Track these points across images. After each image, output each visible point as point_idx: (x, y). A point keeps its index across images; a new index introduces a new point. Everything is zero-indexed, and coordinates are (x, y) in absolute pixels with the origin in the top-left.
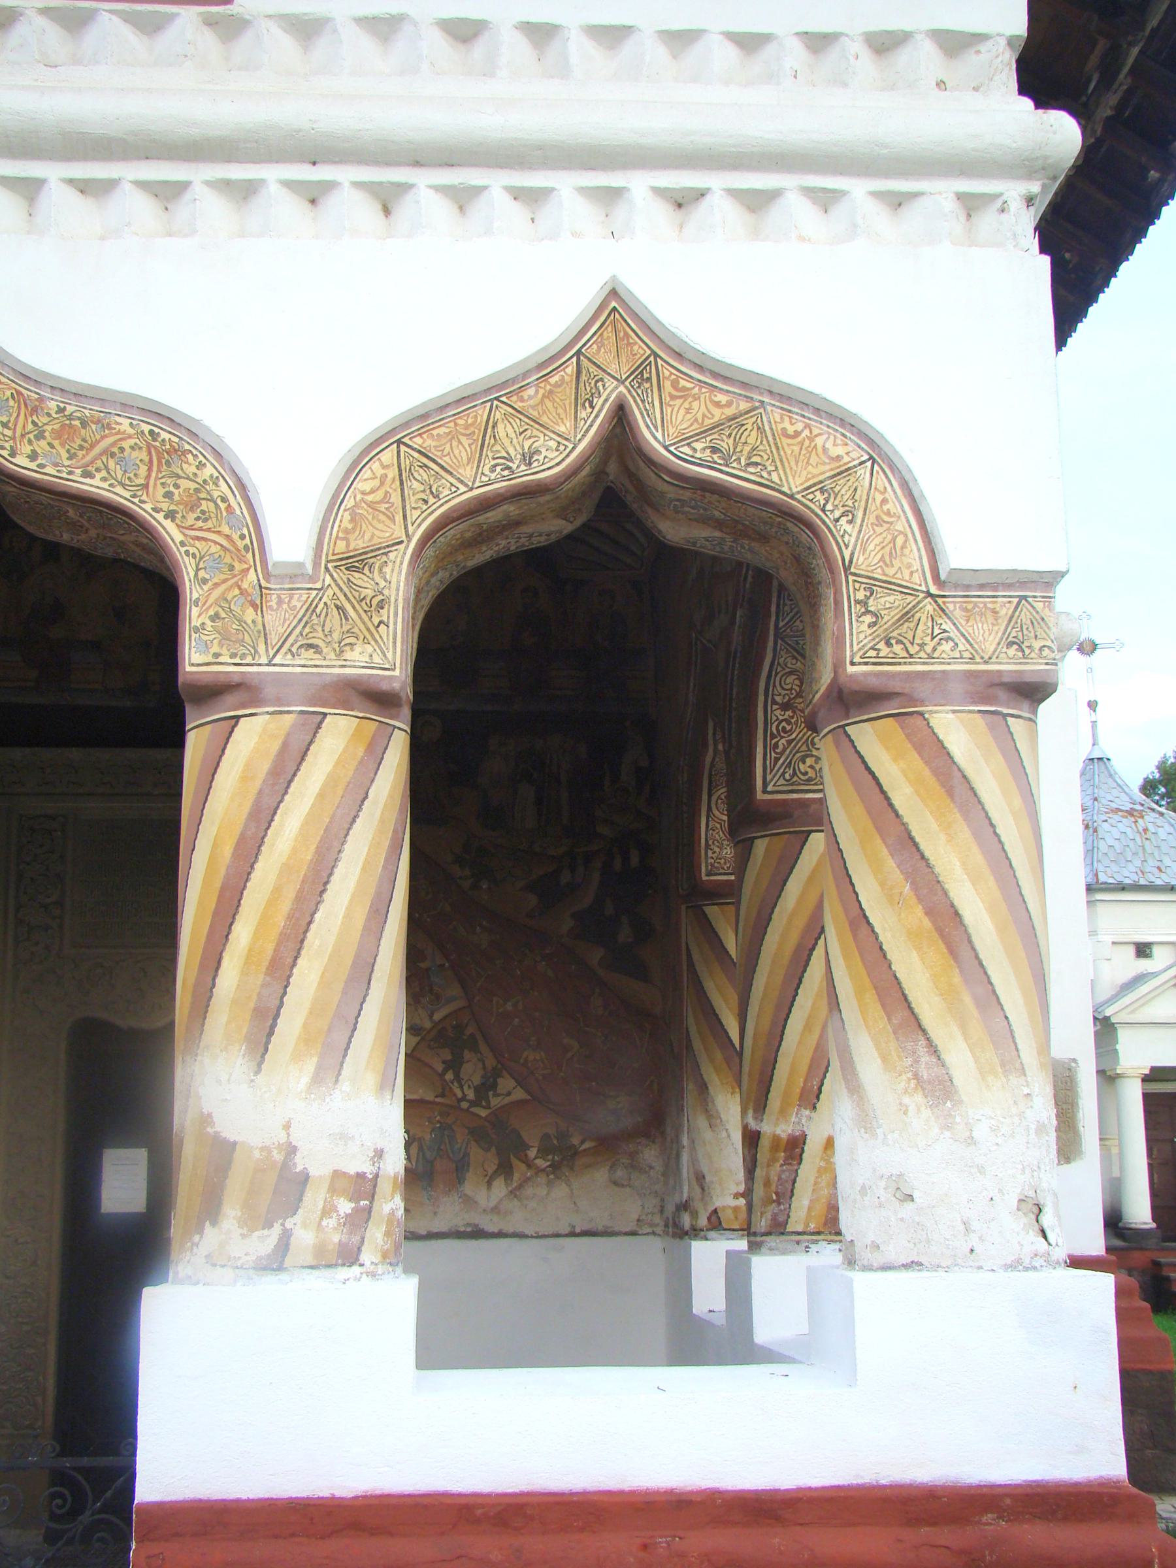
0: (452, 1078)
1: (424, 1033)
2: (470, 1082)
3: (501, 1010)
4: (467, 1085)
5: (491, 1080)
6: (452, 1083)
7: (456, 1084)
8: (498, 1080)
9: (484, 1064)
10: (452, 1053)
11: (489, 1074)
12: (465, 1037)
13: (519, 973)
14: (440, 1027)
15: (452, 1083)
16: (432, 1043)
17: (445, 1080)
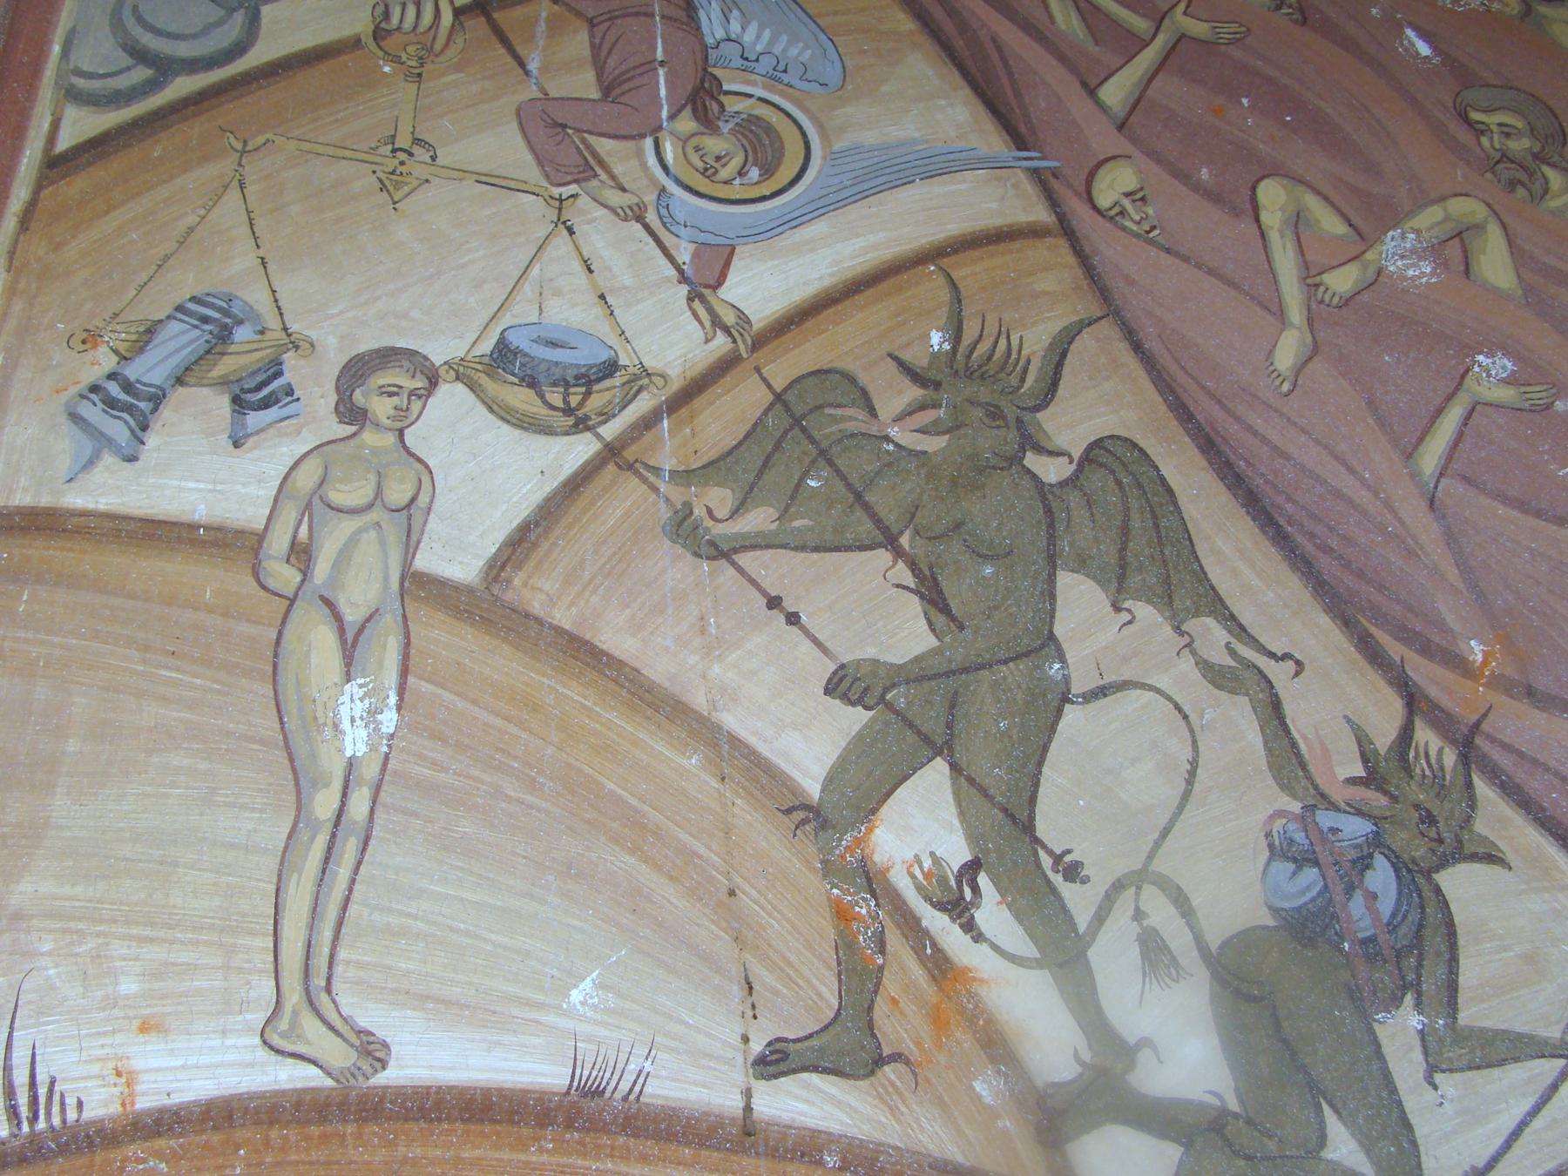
0: (956, 851)
1: (642, 405)
2: (1162, 914)
3: (1342, 281)
4: (1121, 921)
5: (1381, 877)
6: (958, 908)
7: (992, 913)
8: (1445, 879)
9: (1273, 711)
10: (933, 597)
11: (1355, 828)
12: (1052, 471)
13: (1424, 49)
14: (782, 370)
15: (958, 908)
16: (719, 498)
17: (872, 880)
